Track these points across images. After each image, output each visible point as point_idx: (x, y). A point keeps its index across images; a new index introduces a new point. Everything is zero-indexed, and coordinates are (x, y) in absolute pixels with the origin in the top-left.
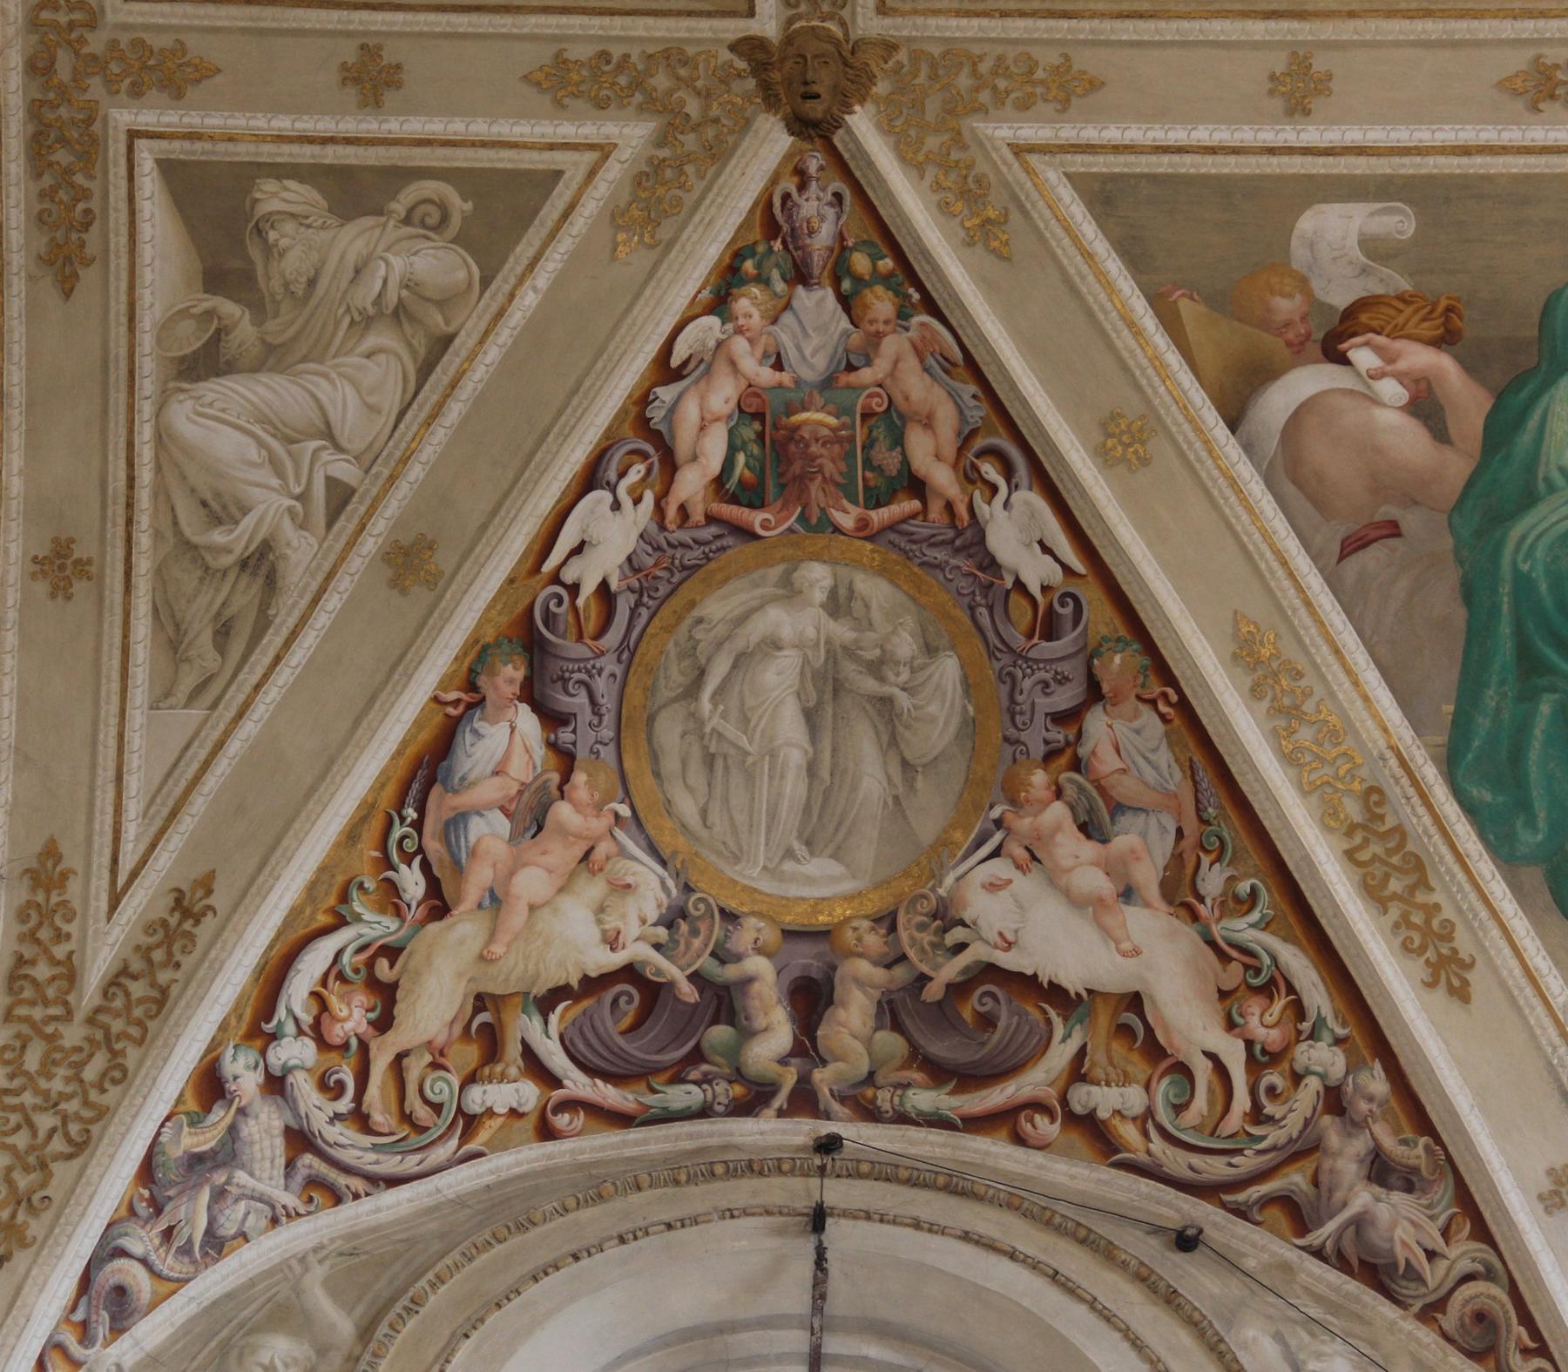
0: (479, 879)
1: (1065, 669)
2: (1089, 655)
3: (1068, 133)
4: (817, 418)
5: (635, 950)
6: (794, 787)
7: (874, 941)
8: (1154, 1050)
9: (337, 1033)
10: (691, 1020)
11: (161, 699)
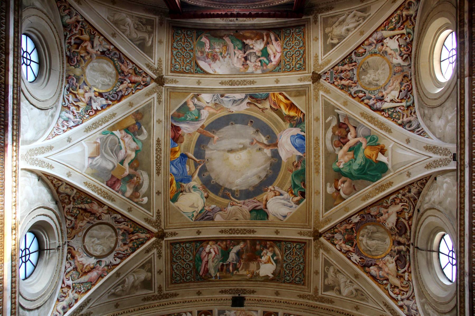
0: (385, 275)
1: (367, 216)
2: (366, 214)
3: (321, 213)
4: (346, 237)
5: (394, 260)
6: (380, 242)
7: (394, 236)
8: (402, 211)
9: (398, 292)
10: (400, 255)
11: (368, 302)
